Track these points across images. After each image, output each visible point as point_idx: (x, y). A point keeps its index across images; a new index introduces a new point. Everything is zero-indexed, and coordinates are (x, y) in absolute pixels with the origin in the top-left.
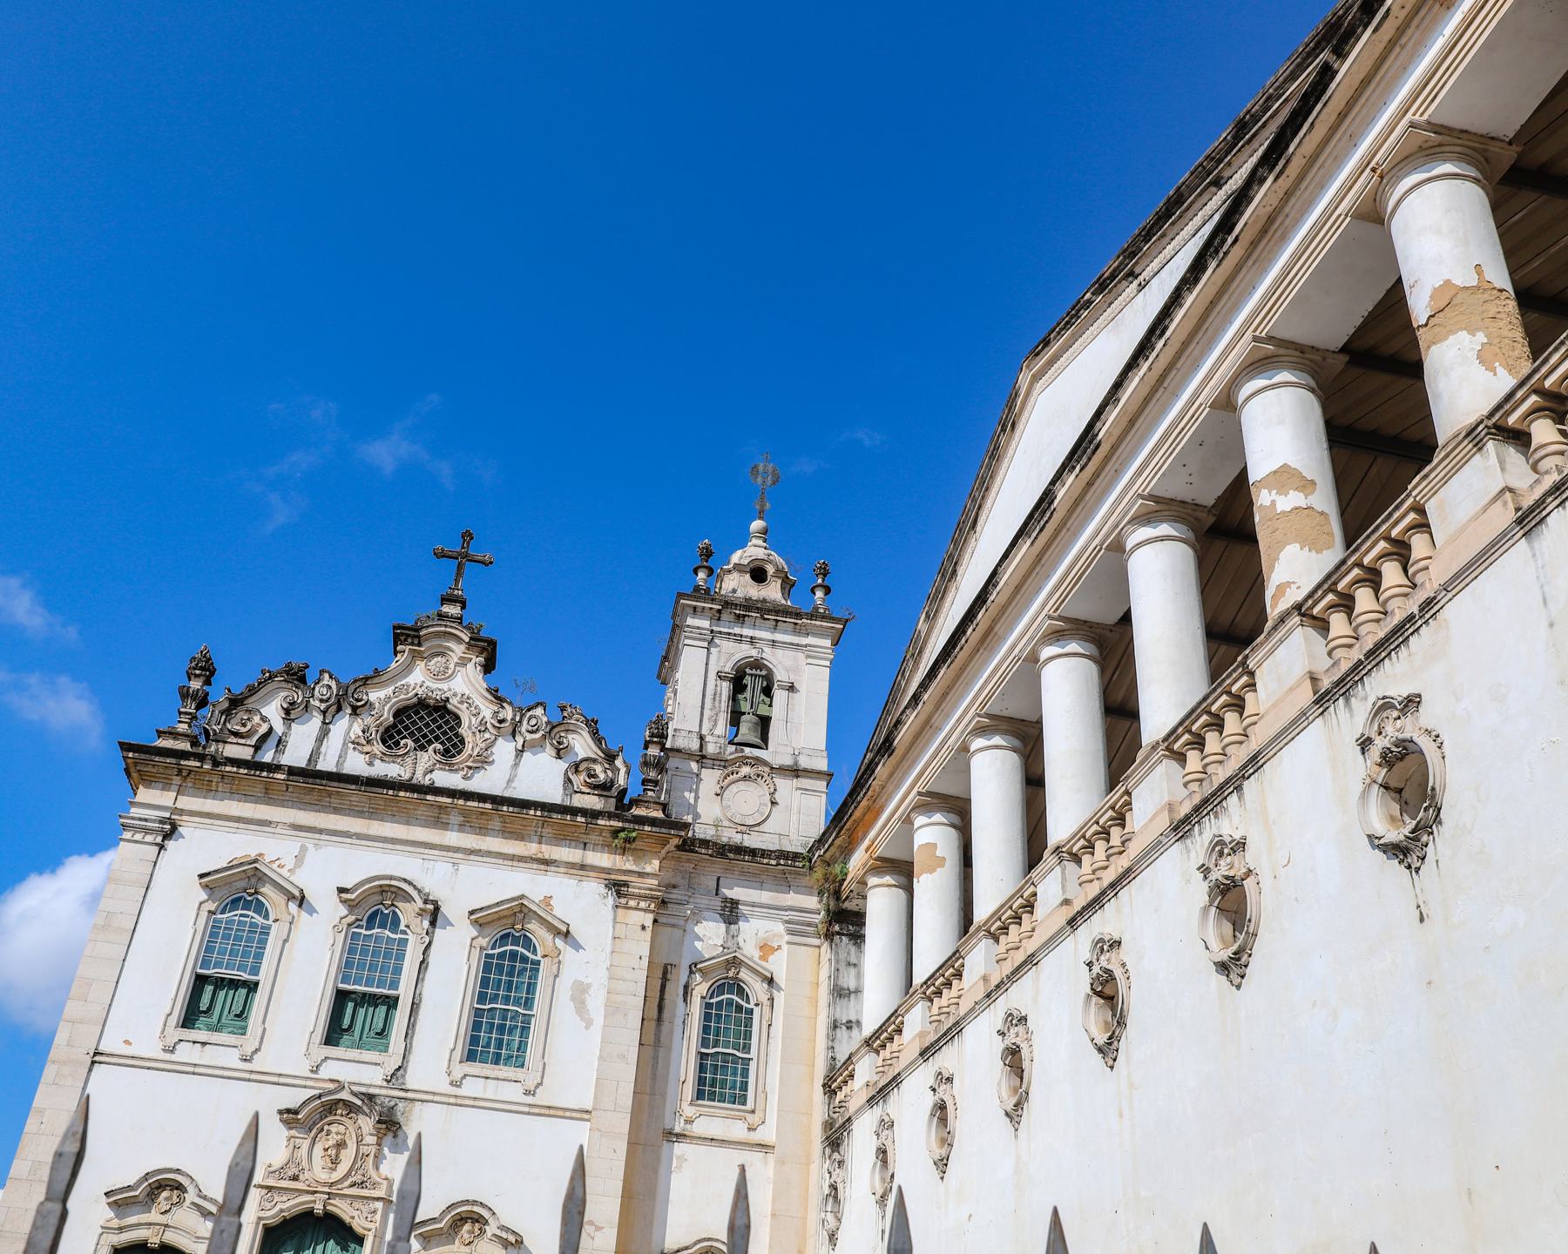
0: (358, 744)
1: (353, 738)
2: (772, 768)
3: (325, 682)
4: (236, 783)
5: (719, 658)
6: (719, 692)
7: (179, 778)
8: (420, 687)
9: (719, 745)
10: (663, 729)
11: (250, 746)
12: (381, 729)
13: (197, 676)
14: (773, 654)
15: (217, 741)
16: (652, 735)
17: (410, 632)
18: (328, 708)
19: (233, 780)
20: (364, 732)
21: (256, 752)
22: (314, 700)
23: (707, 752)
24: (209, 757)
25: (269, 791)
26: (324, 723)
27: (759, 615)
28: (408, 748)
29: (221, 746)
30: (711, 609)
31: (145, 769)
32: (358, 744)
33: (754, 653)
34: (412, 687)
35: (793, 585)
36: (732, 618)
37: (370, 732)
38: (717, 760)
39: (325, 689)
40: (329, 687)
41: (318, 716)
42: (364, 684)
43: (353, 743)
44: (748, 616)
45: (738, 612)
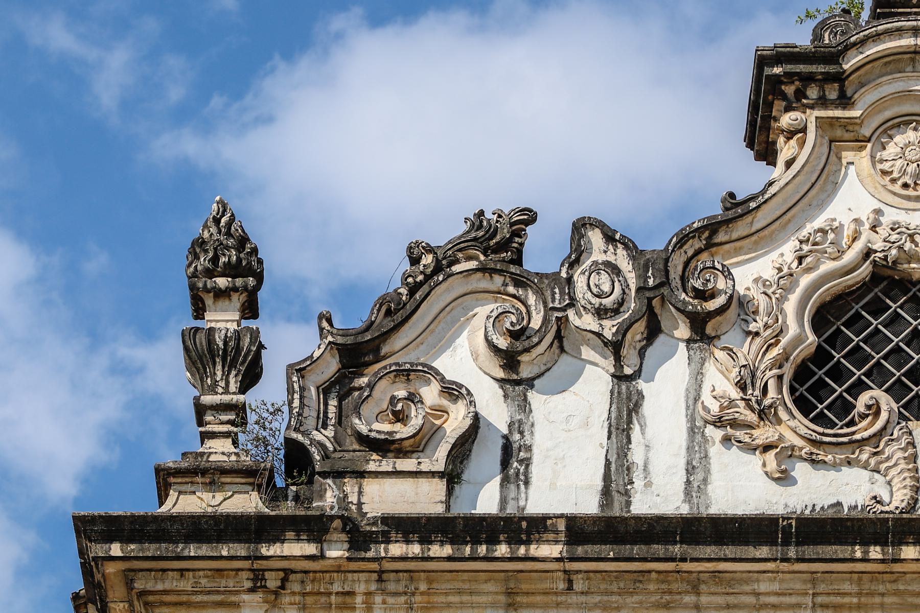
0: (735, 424)
1: (714, 407)
3: (597, 256)
4: (423, 587)
7: (258, 597)
8: (873, 228)
11: (432, 474)
12: (788, 371)
13: (221, 294)
15: (338, 475)
17: (813, 68)
18: (624, 330)
19: (412, 579)
20: (742, 386)
21: (450, 492)
22: (580, 316)
24: (337, 523)
25: (518, 599)
26: (619, 377)
28: (884, 416)
29: (350, 486)
31: (160, 587)
32: (735, 424)
34: (847, 232)
37: (759, 384)
39: (605, 277)
40: (614, 270)
41: (597, 358)
42: (710, 245)
43: (719, 422)
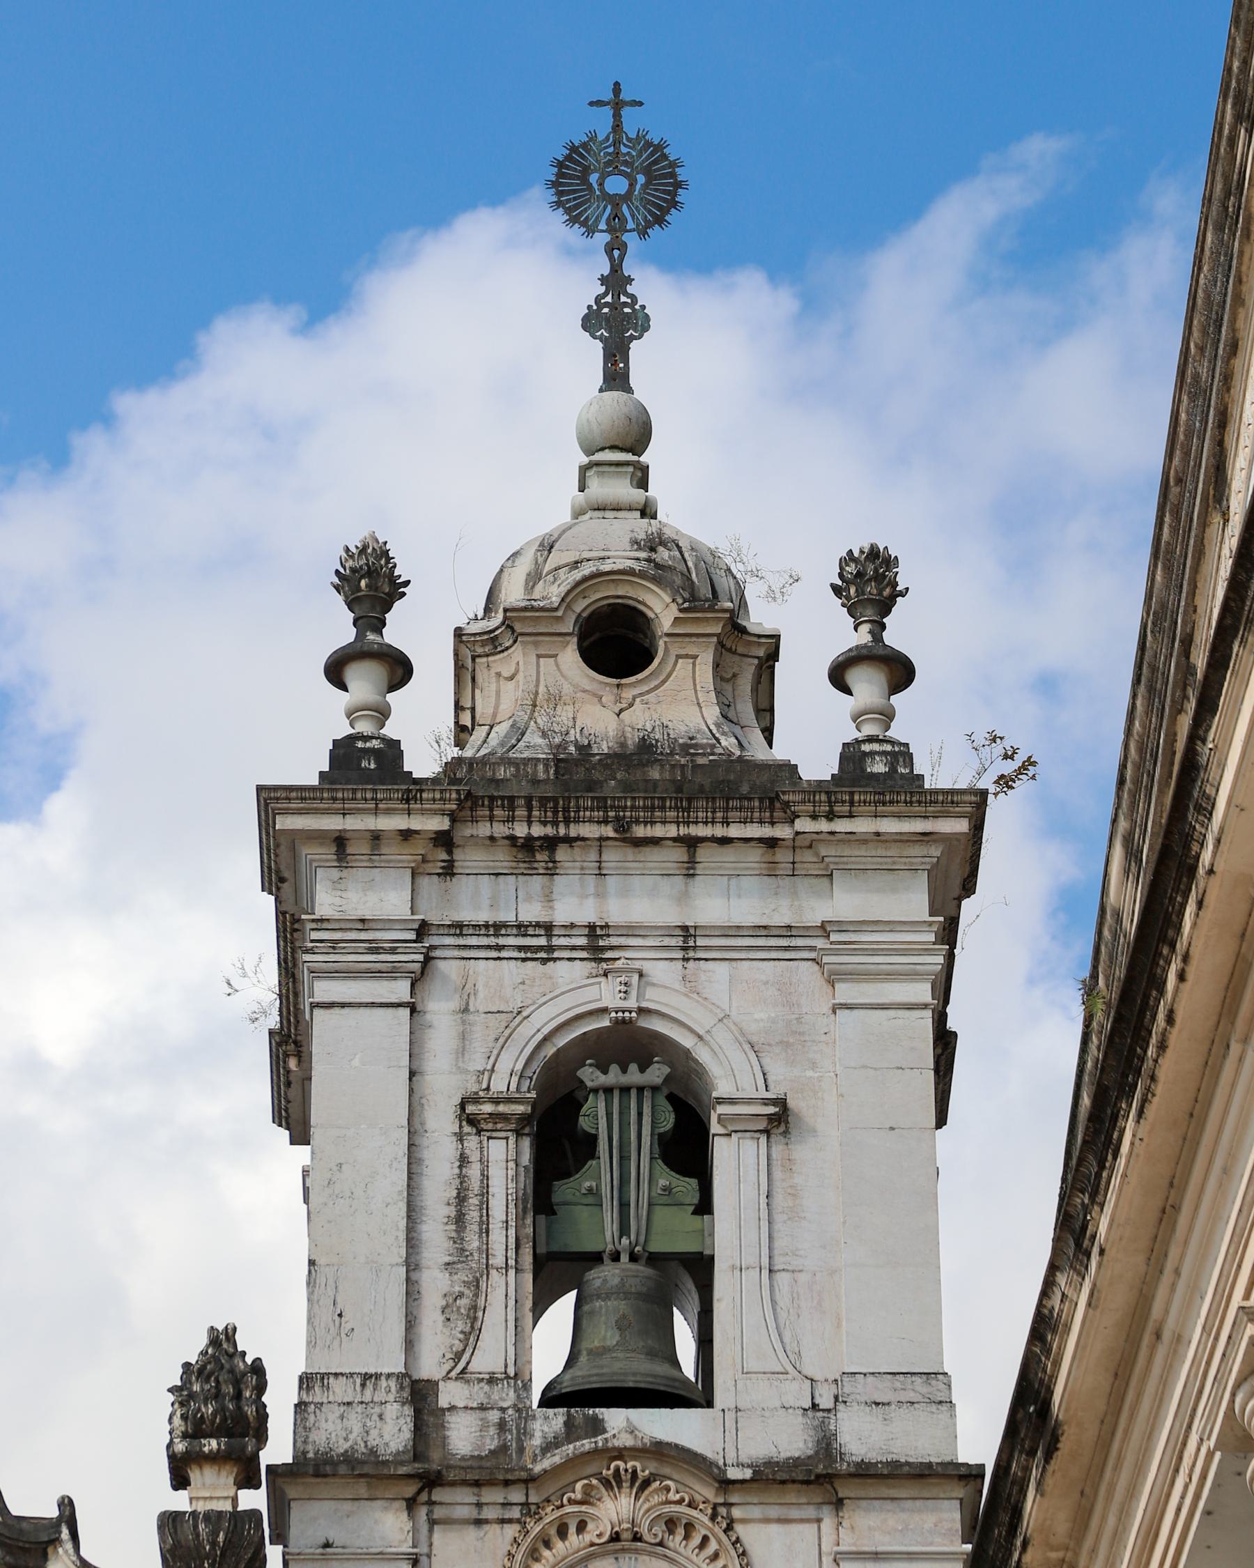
2: (726, 1484)
5: (463, 1037)
6: (475, 1184)
9: (494, 1416)
10: (238, 1396)
14: (691, 987)
16: (196, 1429)
23: (447, 1455)
27: (609, 831)
30: (407, 835)
33: (607, 994)
35: (774, 656)
36: (502, 858)
38: (491, 1483)
44: (569, 841)
45: (520, 830)
